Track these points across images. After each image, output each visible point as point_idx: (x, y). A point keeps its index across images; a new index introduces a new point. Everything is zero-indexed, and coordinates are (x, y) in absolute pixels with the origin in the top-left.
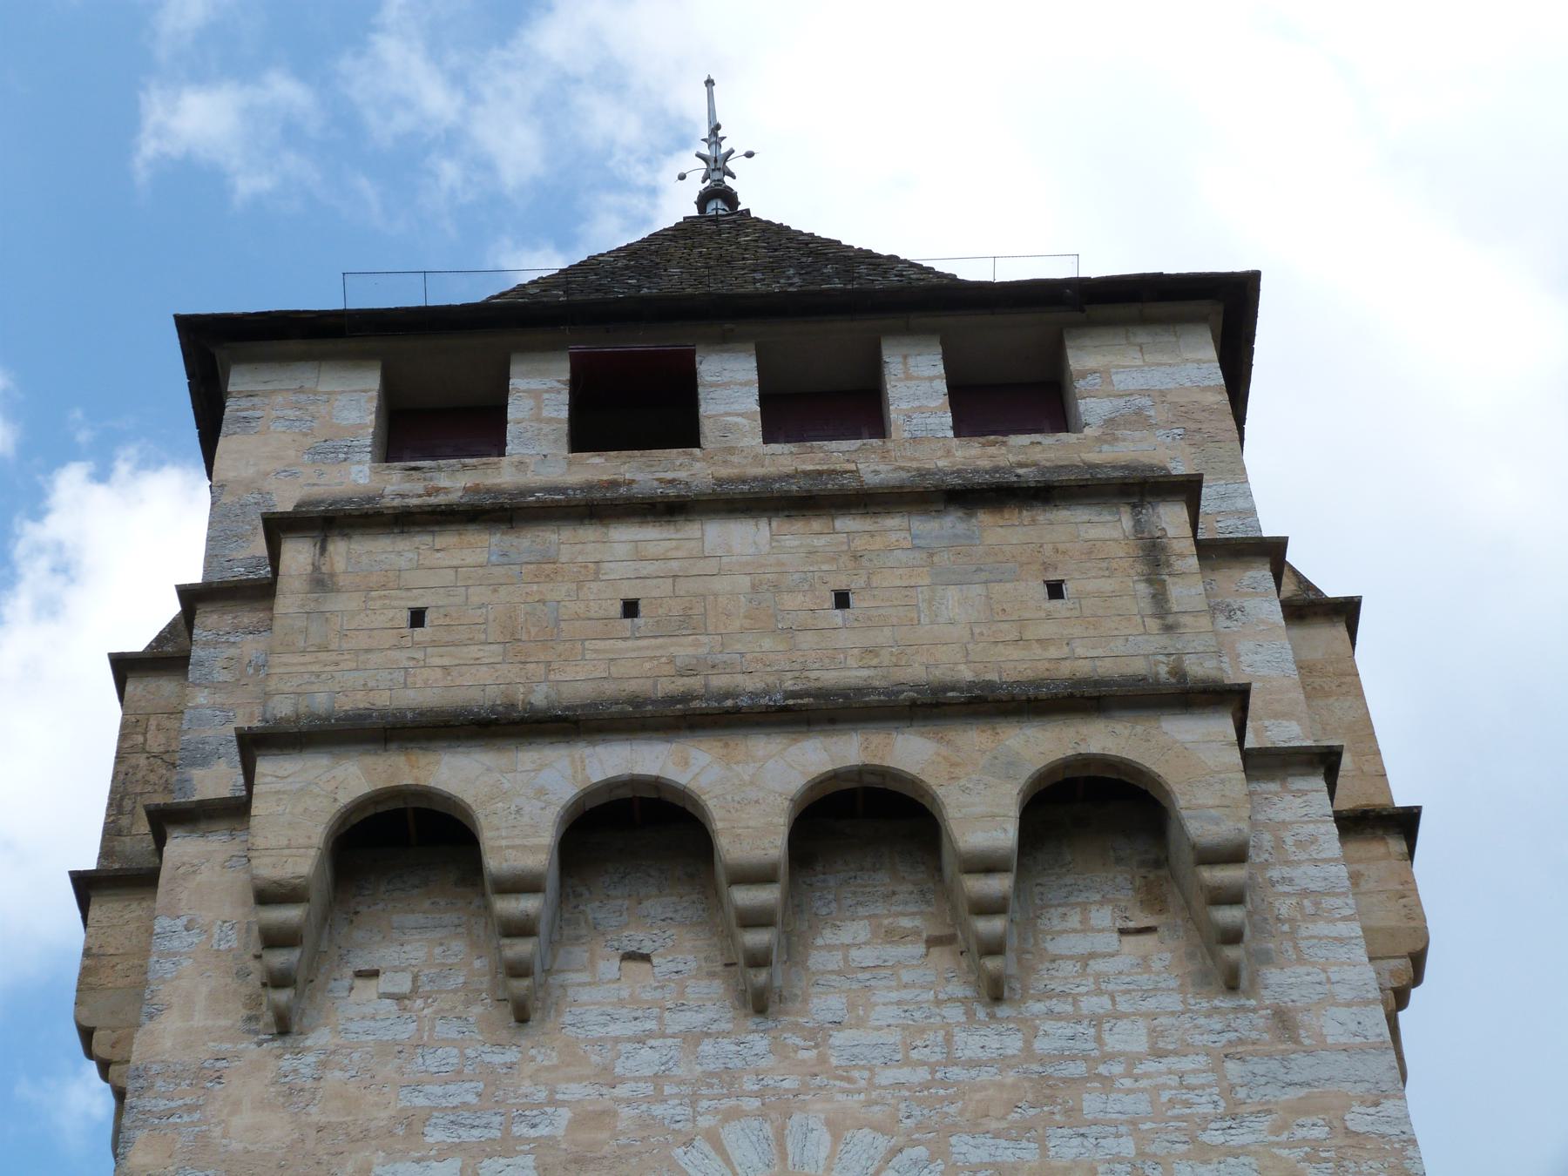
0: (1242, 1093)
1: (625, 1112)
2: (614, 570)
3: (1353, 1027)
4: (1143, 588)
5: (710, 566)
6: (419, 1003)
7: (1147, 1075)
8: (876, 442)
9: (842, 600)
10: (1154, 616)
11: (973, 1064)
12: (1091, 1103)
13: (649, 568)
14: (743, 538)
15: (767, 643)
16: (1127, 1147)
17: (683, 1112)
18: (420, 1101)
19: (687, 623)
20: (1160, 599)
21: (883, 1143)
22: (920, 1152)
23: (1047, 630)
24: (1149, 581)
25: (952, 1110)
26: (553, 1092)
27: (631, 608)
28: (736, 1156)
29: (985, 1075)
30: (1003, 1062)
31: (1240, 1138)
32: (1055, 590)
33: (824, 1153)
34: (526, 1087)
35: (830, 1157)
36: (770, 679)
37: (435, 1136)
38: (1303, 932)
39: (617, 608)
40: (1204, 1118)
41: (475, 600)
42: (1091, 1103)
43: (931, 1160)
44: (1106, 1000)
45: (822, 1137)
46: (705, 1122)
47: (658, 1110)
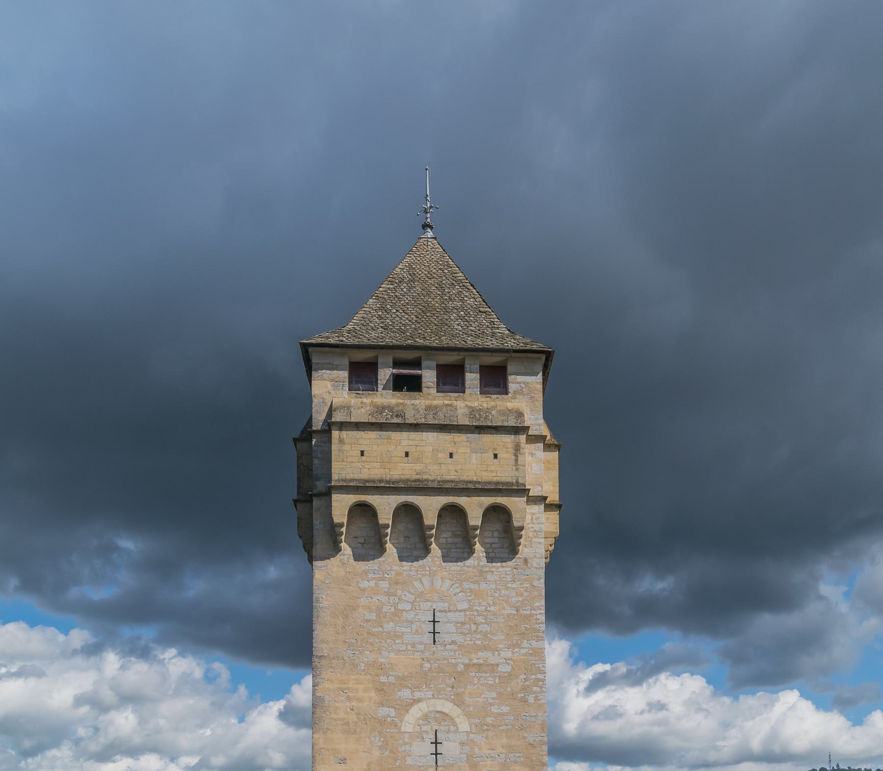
2: (405, 442)
11: (469, 567)
12: (489, 577)
16: (494, 586)
20: (516, 460)
21: (451, 583)
23: (493, 468)
29: (471, 569)
30: (474, 567)
31: (514, 586)
32: (496, 456)
37: (371, 576)
42: (489, 577)
45: (440, 580)
46: (419, 576)
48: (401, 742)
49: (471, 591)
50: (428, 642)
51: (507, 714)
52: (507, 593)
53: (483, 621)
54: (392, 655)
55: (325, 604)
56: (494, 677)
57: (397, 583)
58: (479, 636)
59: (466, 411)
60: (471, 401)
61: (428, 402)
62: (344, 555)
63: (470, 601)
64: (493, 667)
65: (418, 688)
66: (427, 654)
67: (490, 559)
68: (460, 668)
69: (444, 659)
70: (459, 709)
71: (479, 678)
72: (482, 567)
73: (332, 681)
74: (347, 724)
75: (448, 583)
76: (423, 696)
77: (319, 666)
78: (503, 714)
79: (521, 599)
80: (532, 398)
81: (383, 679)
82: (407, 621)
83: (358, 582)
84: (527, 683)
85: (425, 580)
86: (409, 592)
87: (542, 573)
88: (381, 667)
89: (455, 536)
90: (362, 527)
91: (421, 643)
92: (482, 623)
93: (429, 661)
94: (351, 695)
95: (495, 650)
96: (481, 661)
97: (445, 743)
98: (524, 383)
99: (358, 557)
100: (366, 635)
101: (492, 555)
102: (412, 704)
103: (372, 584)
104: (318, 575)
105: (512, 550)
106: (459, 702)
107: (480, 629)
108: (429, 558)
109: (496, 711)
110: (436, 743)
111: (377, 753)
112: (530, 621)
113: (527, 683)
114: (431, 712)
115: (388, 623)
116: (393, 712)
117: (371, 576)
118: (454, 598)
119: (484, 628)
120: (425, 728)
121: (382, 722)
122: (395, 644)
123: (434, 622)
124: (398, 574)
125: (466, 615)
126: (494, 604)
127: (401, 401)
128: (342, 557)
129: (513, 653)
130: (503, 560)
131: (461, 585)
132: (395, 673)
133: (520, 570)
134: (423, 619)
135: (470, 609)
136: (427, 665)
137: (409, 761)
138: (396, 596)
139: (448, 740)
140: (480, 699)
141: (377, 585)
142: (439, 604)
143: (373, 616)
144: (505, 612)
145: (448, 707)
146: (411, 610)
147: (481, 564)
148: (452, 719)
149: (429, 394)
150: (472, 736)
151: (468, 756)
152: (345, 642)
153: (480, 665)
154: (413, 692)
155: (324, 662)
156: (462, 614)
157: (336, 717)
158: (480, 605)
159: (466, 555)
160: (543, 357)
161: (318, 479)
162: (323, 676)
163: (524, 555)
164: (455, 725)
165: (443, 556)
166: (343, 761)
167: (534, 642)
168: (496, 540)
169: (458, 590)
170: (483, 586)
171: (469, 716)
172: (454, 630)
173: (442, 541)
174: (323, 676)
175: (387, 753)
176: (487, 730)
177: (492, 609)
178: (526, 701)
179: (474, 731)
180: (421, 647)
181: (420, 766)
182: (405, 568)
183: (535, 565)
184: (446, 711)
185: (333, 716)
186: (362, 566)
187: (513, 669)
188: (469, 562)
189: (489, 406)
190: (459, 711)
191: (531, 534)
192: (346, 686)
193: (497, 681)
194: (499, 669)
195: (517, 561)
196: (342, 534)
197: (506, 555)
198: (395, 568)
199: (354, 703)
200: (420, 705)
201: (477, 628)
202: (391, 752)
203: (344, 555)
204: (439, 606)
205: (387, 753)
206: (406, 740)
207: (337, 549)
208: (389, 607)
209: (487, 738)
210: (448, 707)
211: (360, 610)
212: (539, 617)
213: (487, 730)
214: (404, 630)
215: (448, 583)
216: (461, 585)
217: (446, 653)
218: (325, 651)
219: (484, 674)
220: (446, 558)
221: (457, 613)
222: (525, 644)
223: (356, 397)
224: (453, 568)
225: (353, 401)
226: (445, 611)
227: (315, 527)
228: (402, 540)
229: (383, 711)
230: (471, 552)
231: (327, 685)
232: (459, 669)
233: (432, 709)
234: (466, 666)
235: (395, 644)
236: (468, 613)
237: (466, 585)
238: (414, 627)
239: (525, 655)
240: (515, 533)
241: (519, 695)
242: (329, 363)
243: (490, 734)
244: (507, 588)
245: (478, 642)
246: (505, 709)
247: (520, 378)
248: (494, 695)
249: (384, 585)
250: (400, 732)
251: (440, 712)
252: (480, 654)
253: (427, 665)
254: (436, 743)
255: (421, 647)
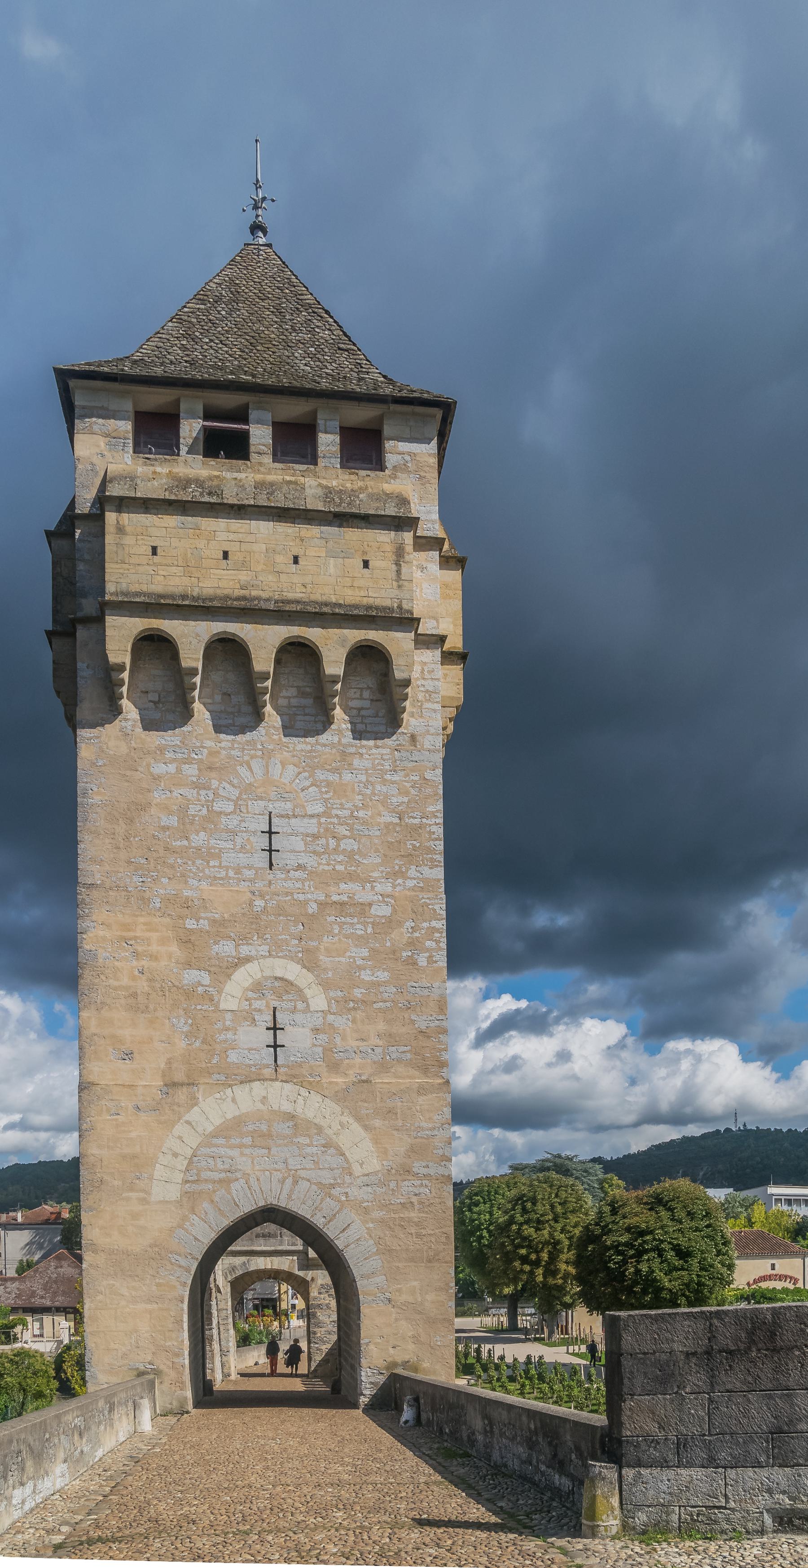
0: (398, 762)
1: (224, 752)
3: (432, 743)
4: (394, 567)
5: (250, 538)
6: (161, 705)
7: (373, 754)
8: (312, 467)
9: (296, 560)
10: (396, 580)
11: (325, 745)
12: (356, 762)
13: (232, 537)
14: (264, 529)
15: (270, 578)
16: (363, 778)
17: (239, 754)
18: (163, 742)
19: (244, 565)
22: (306, 774)
24: (396, 564)
25: (316, 761)
26: (202, 743)
27: (226, 555)
28: (255, 771)
29: (327, 750)
30: (333, 746)
31: (396, 778)
33: (280, 772)
34: (194, 740)
35: (281, 774)
36: (271, 594)
37: (169, 755)
38: (424, 706)
39: (221, 555)
40: (387, 771)
41: (173, 544)
42: (356, 762)
43: (309, 777)
44: (364, 726)
45: (279, 766)
46: (246, 758)
47: (233, 752)
48: (219, 1025)
49: (329, 784)
50: (261, 865)
51: (385, 983)
52: (384, 789)
53: (347, 833)
54: (204, 885)
55: (96, 799)
56: (365, 924)
57: (210, 768)
58: (340, 858)
59: (320, 492)
60: (327, 477)
61: (259, 477)
62: (126, 720)
63: (326, 800)
64: (364, 908)
65: (244, 939)
66: (259, 885)
67: (358, 734)
68: (313, 908)
69: (287, 894)
70: (310, 975)
71: (341, 925)
72: (345, 746)
73: (109, 926)
74: (134, 995)
75: (291, 770)
76: (253, 953)
77: (88, 900)
78: (379, 984)
79: (406, 799)
80: (421, 478)
81: (190, 924)
82: (228, 831)
83: (148, 765)
84: (417, 934)
85: (256, 765)
86: (231, 783)
87: (438, 758)
88: (187, 904)
89: (302, 694)
90: (155, 674)
91: (249, 867)
92: (345, 837)
93: (262, 896)
94: (140, 949)
95: (366, 881)
96: (345, 898)
97: (288, 1028)
98: (409, 454)
99: (149, 725)
100: (162, 852)
101: (360, 727)
102: (236, 966)
103: (172, 768)
104: (85, 753)
105: (392, 720)
106: (310, 963)
107: (343, 846)
108: (261, 729)
109: (367, 978)
110: (275, 1029)
111: (182, 1044)
112: (420, 835)
113: (417, 934)
114: (266, 978)
115: (197, 833)
116: (206, 979)
117: (169, 755)
118: (302, 795)
119: (349, 845)
120: (257, 1004)
121: (189, 993)
122: (209, 867)
123: (270, 833)
124: (213, 753)
125: (320, 824)
126: (365, 807)
127: (216, 473)
128: (123, 724)
129: (394, 886)
130: (377, 736)
131: (312, 775)
132: (209, 915)
133: (404, 754)
134: (253, 827)
135: (327, 814)
136: (259, 903)
137: (233, 1057)
138: (208, 788)
139: (294, 1024)
140: (343, 960)
141: (179, 770)
142: (277, 804)
143: (173, 821)
144: (382, 820)
145: (292, 971)
146: (234, 812)
147: (344, 741)
148: (300, 991)
149: (260, 464)
150: (330, 1018)
151: (325, 1050)
152: (129, 862)
153: (342, 904)
154: (237, 946)
155: (95, 894)
156: (314, 821)
157: (116, 983)
158: (342, 807)
159: (319, 726)
160: (439, 413)
161: (85, 595)
162: (94, 918)
163: (411, 730)
164: (305, 1000)
165: (284, 727)
166: (129, 1055)
167: (426, 868)
168: (367, 704)
169: (307, 783)
170: (347, 777)
171: (326, 985)
172: (301, 846)
173: (282, 702)
174: (94, 918)
175: (198, 1044)
176: (354, 1009)
177: (361, 814)
178: (415, 963)
179: (334, 1010)
180: (249, 874)
181: (250, 1066)
182: (223, 745)
183: (427, 745)
184: (290, 977)
185: (113, 982)
186: (155, 739)
187: (394, 911)
188: (324, 738)
189: (356, 487)
190: (310, 977)
191: (421, 696)
192: (131, 934)
193: (370, 930)
194: (373, 911)
195: (399, 738)
196: (122, 684)
197: (382, 728)
198: (209, 743)
199: (145, 963)
200: (249, 966)
201: (338, 845)
202: (204, 1042)
203: (126, 720)
204: (278, 807)
205: (198, 1044)
206: (228, 1023)
207: (116, 711)
208: (198, 808)
209: (354, 1021)
210: (292, 971)
211: (153, 811)
212: (434, 828)
213: (354, 1009)
214: (223, 845)
215: (291, 770)
216: (312, 775)
217: (289, 884)
218: (98, 876)
219: (348, 919)
220: (289, 730)
221: (306, 820)
222: (412, 872)
223: (145, 464)
224: (299, 747)
225: (140, 469)
226: (287, 816)
227: (80, 673)
228: (218, 698)
229: (191, 976)
230: (327, 721)
231: (101, 932)
232: (310, 911)
233: (267, 973)
234: (322, 905)
235: (209, 867)
236: (323, 820)
237: (320, 775)
238: (239, 840)
239: (413, 889)
240: (397, 691)
241: (404, 954)
242: (102, 408)
243: (359, 1015)
244: (384, 782)
245: (340, 868)
246: (383, 976)
247: (403, 446)
248: (365, 952)
249: (191, 771)
250: (217, 1010)
251: (281, 979)
252: (343, 886)
253: (259, 903)
254: (275, 1029)
255: (249, 874)
